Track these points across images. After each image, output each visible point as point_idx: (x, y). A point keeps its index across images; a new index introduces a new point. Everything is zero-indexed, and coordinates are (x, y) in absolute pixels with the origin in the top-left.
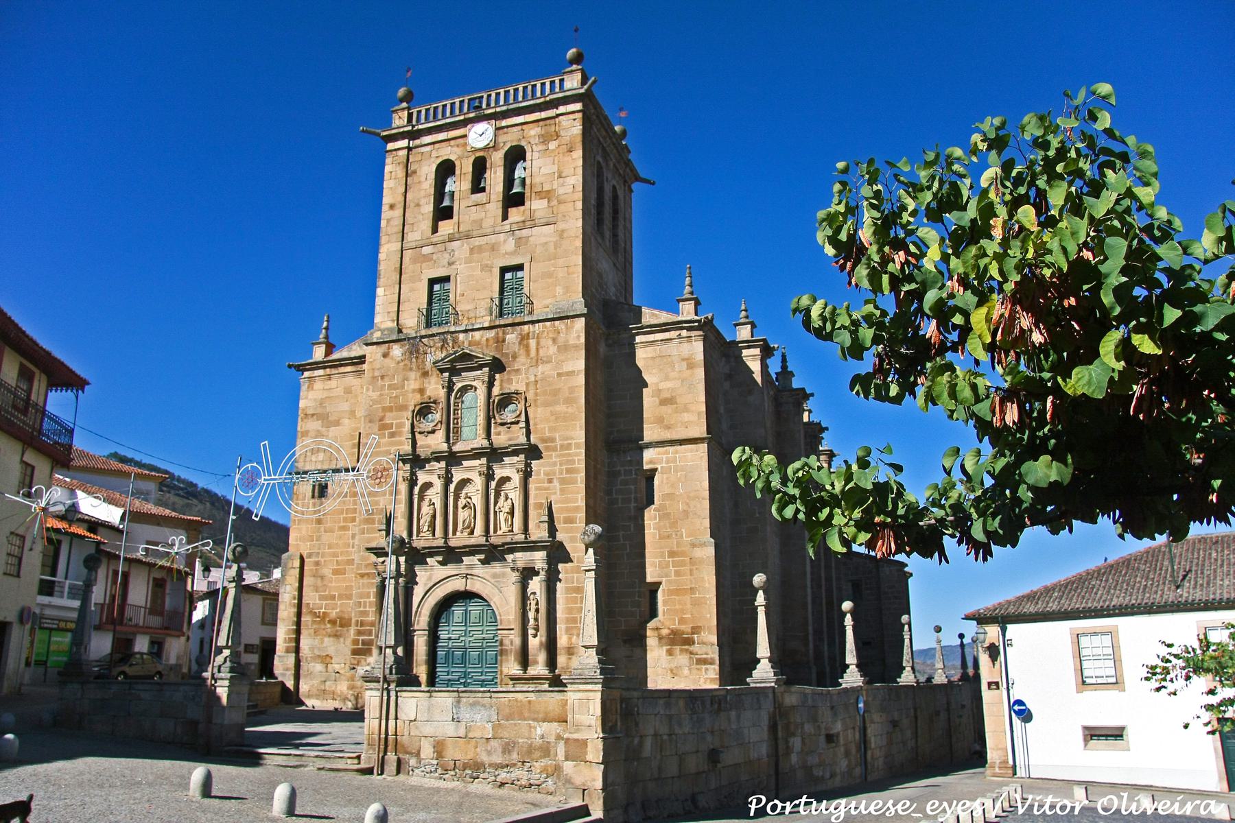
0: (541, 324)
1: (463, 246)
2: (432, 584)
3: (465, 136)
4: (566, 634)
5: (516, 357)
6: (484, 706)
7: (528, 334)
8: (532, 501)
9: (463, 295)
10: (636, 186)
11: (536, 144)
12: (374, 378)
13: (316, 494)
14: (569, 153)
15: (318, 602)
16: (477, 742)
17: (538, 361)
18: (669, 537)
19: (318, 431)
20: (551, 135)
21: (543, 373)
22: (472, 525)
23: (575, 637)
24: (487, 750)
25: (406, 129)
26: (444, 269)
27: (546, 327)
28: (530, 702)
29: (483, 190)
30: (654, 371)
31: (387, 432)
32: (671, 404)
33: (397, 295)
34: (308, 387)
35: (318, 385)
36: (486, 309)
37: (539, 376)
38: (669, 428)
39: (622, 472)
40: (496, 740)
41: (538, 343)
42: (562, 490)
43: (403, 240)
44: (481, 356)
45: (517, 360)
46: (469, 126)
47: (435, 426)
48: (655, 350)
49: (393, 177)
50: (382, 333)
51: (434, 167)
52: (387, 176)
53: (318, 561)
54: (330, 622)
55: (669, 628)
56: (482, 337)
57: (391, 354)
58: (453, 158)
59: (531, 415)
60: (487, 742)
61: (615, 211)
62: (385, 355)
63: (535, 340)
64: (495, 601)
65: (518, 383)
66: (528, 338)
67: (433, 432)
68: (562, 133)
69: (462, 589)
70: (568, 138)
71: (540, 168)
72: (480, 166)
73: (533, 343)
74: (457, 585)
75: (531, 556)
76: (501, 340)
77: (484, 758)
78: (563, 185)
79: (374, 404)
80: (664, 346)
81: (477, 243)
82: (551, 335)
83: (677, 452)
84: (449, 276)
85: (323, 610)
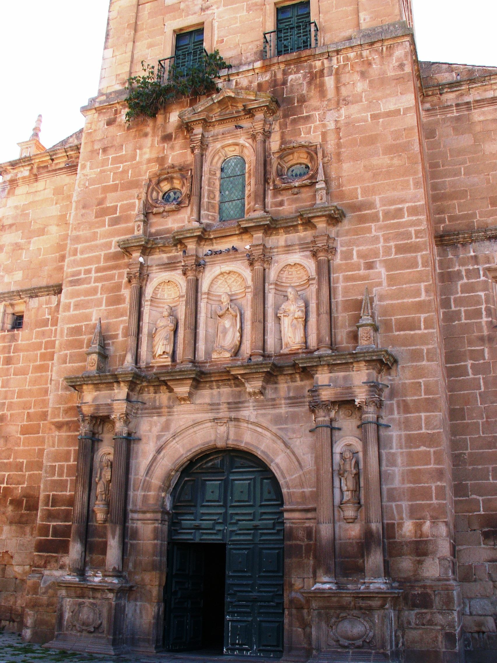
4: (411, 517)
5: (305, 101)
7: (322, 71)
9: (222, 41)
19: (16, 244)
21: (348, 117)
23: (428, 523)
26: (195, 16)
27: (347, 59)
31: (107, 218)
39: (464, 273)
41: (338, 81)
42: (391, 280)
44: (253, 98)
50: (107, 98)
54: (12, 502)
56: (251, 82)
59: (333, 175)
62: (110, 123)
63: (333, 77)
65: (309, 133)
73: (329, 82)
76: (279, 82)
79: (90, 184)
82: (358, 69)
84: (203, 23)
85: (5, 485)
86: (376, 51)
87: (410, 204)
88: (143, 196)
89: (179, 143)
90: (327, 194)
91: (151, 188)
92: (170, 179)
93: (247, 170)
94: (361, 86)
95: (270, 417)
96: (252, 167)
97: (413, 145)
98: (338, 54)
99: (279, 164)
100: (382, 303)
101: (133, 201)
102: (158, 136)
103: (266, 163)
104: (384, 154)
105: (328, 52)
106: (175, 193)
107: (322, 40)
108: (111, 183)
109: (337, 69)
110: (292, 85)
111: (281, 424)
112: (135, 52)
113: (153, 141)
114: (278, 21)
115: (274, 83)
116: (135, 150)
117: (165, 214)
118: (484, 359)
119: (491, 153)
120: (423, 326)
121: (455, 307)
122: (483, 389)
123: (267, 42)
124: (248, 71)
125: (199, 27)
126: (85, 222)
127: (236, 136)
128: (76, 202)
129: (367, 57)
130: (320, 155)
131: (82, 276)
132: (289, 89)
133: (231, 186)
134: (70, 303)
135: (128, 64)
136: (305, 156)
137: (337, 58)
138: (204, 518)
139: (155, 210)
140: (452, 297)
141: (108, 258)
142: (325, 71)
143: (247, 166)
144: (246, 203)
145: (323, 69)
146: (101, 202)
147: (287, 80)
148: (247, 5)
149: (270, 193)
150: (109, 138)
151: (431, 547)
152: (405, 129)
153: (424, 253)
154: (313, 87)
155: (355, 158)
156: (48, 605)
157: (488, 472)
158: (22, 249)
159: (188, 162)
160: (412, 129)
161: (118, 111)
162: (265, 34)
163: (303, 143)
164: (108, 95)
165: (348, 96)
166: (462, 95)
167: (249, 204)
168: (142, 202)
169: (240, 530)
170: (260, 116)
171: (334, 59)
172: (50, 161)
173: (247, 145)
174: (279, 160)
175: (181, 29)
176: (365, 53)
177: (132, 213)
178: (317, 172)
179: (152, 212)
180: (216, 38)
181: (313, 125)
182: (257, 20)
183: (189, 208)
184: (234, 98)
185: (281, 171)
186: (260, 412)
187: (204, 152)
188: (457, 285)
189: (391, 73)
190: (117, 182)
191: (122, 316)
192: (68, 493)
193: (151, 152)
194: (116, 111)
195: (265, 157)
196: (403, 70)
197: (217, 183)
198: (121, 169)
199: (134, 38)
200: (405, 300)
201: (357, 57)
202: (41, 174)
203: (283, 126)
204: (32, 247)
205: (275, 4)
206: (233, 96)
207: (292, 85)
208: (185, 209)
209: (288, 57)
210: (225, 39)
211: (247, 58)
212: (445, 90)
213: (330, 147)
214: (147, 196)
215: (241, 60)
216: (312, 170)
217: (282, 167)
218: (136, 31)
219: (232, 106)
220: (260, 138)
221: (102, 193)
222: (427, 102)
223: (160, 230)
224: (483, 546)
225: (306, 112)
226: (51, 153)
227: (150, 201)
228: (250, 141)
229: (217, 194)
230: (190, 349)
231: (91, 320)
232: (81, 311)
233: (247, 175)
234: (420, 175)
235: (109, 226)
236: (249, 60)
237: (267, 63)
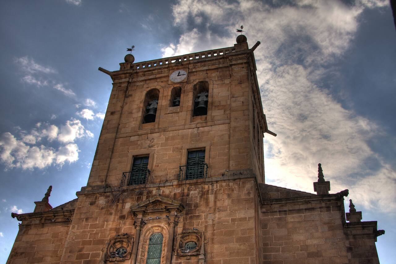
1: (161, 136)
3: (168, 76)
5: (198, 207)
11: (216, 81)
17: (216, 209)
21: (219, 218)
25: (128, 72)
27: (221, 186)
30: (301, 231)
32: (318, 257)
41: (216, 198)
44: (171, 203)
48: (301, 216)
50: (92, 189)
51: (144, 93)
57: (97, 203)
58: (158, 87)
59: (209, 250)
63: (213, 195)
65: (198, 225)
66: (208, 194)
72: (177, 93)
73: (211, 197)
76: (185, 194)
78: (235, 101)
79: (76, 239)
80: (308, 214)
81: (171, 135)
82: (226, 192)
84: (149, 154)
86: (237, 184)
88: (105, 250)
89: (129, 221)
90: (205, 261)
91: (110, 245)
92: (121, 242)
94: (227, 202)
96: (166, 241)
97: (252, 238)
98: (217, 183)
99: (181, 241)
101: (99, 252)
102: (118, 215)
103: (174, 240)
104: (237, 242)
105: (212, 181)
106: (123, 250)
107: (210, 174)
108: (88, 239)
109: (216, 191)
110: (192, 197)
112: (111, 164)
113: (115, 218)
114: (188, 159)
115: (183, 194)
116: (104, 222)
117: (116, 262)
119: (296, 240)
123: (181, 170)
124: (170, 186)
125: (147, 156)
126: (70, 261)
127: (160, 222)
128: (66, 248)
129: (232, 186)
130: (203, 239)
132: (190, 199)
133: (154, 249)
135: (106, 171)
136: (195, 238)
137: (217, 185)
139: (110, 259)
142: (210, 191)
143: (164, 239)
144: (161, 261)
145: (209, 190)
146: (81, 250)
147: (189, 194)
148: (173, 147)
149: (174, 257)
150: (91, 212)
152: (248, 229)
154: (202, 199)
155: (221, 242)
159: (133, 233)
160: (252, 229)
161: (97, 198)
162: (180, 167)
164: (93, 187)
165: (220, 207)
166: (282, 206)
167: (163, 262)
168: (104, 253)
170: (174, 213)
171: (215, 185)
172: (53, 217)
173: (165, 228)
174: (181, 239)
175: (137, 156)
176: (231, 184)
177: (98, 259)
178: (200, 248)
179: (109, 260)
180: (155, 164)
181: (201, 221)
182: (177, 157)
183: (130, 261)
184: (161, 201)
185: (182, 244)
187: (142, 229)
189: (243, 197)
190: (92, 239)
193: (113, 224)
194: (96, 197)
195: (174, 235)
196: (250, 196)
197: (147, 247)
198: (94, 232)
199: (111, 157)
201: (226, 185)
202: (46, 223)
203: (185, 219)
205: (188, 149)
206: (160, 200)
207: (192, 197)
208: (127, 261)
209: (191, 181)
210: (160, 165)
211: (170, 177)
212: (274, 203)
213: (209, 234)
214: (107, 250)
215: (167, 178)
216: (198, 246)
217: (183, 243)
218: (112, 152)
219: (159, 204)
220: (172, 225)
221: (82, 245)
222: (264, 208)
225: (198, 213)
226: (55, 212)
227: (109, 254)
228: (167, 225)
229: (146, 253)
233: (163, 245)
234: (255, 256)
236: (171, 179)
237: (180, 183)
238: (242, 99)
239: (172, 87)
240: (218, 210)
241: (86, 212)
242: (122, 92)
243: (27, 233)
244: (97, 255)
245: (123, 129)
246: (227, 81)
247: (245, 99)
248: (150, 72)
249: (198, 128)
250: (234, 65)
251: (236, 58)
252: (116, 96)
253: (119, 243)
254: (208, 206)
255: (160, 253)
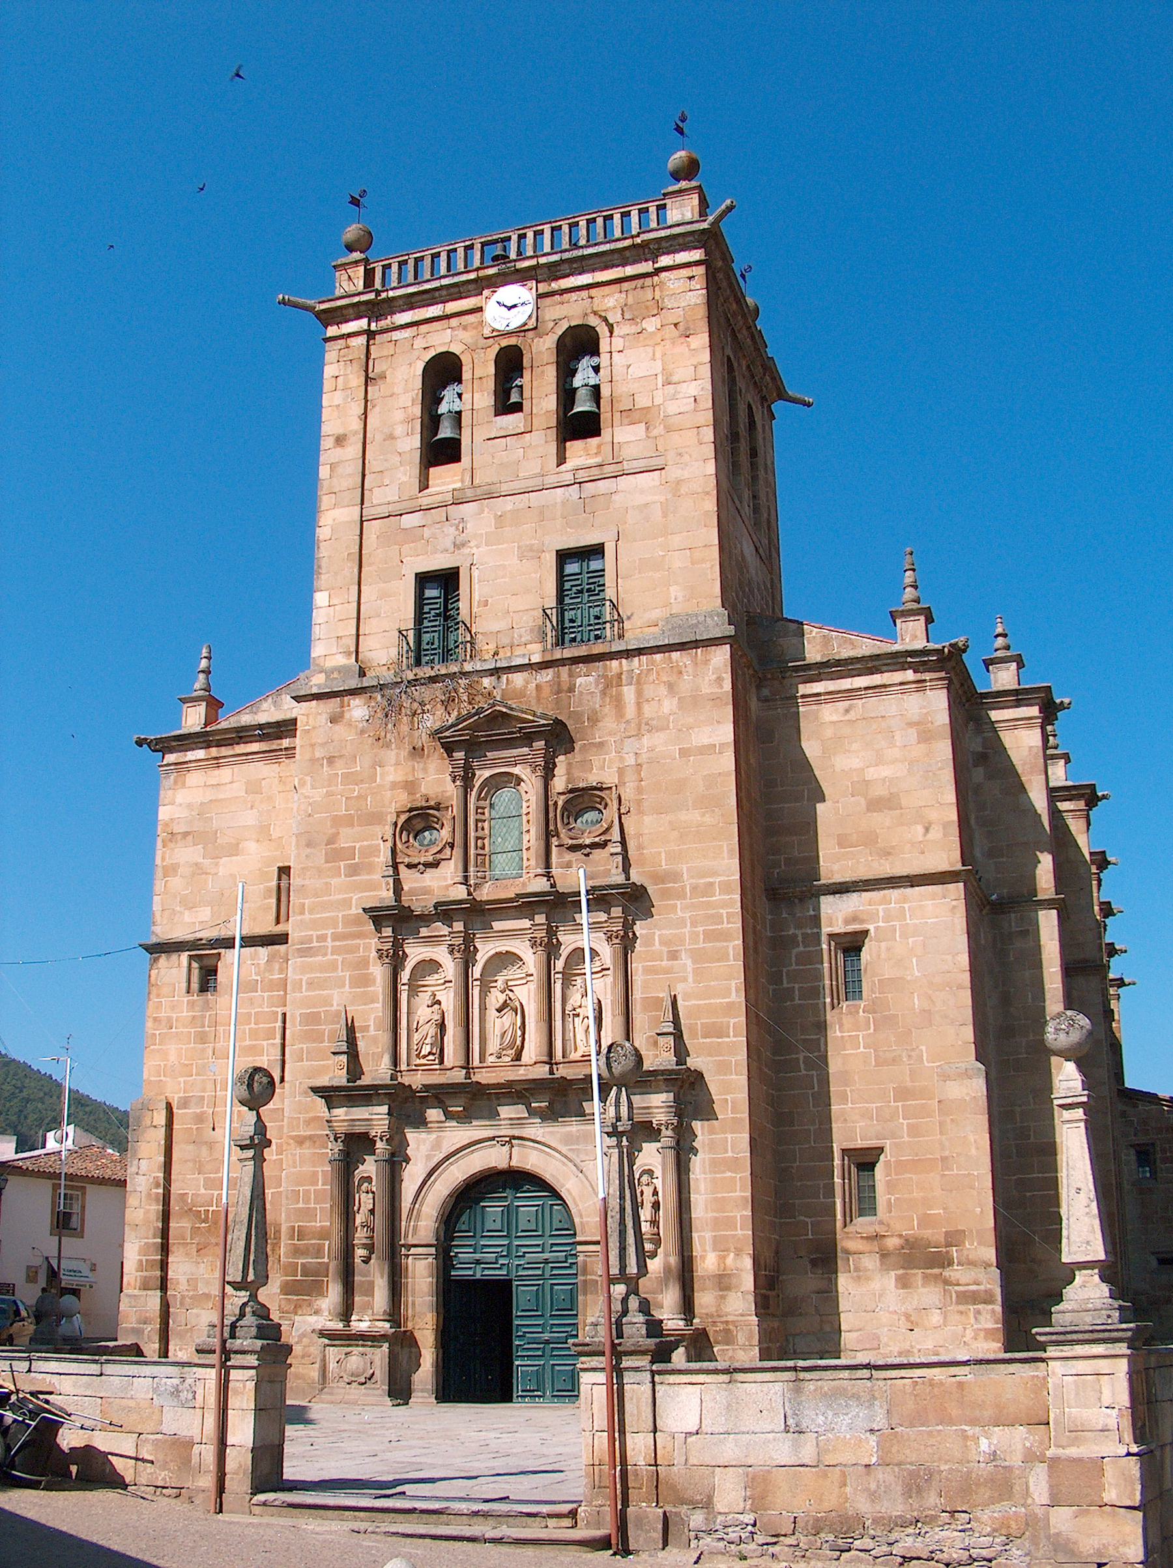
0: (644, 658)
2: (442, 1156)
3: (480, 309)
6: (856, 1397)
7: (620, 675)
8: (637, 994)
9: (486, 604)
10: (778, 407)
12: (313, 760)
13: (195, 986)
14: (683, 340)
15: (203, 1191)
16: (843, 1474)
17: (643, 726)
18: (894, 1061)
19: (196, 864)
20: (647, 307)
22: (519, 1042)
24: (867, 1489)
28: (960, 1385)
29: (517, 408)
30: (855, 746)
31: (342, 864)
32: (890, 809)
33: (355, 604)
34: (176, 782)
35: (195, 778)
36: (532, 631)
37: (644, 758)
38: (889, 854)
39: (800, 938)
40: (888, 1469)
41: (639, 693)
43: (362, 503)
44: (531, 718)
45: (600, 724)
46: (486, 292)
47: (440, 852)
49: (340, 386)
50: (327, 677)
51: (420, 367)
52: (327, 385)
53: (203, 1113)
55: (900, 1236)
57: (347, 715)
58: (456, 349)
59: (630, 830)
60: (868, 1474)
61: (754, 453)
62: (334, 720)
63: (633, 688)
64: (568, 1186)
65: (603, 768)
67: (435, 865)
68: (668, 303)
69: (502, 1164)
70: (680, 312)
71: (629, 367)
74: (494, 1158)
75: (643, 1100)
77: (863, 1506)
78: (674, 398)
81: (509, 507)
83: (905, 900)
85: (214, 1208)
87: (722, 878)
93: (524, 811)
94: (669, 705)
95: (558, 1136)
97: (728, 798)
100: (687, 1003)
101: (377, 842)
105: (627, 650)
110: (581, 693)
111: (572, 1144)
113: (398, 755)
118: (819, 1051)
120: (732, 1034)
121: (788, 983)
122: (816, 1089)
131: (315, 944)
133: (505, 830)
134: (301, 979)
138: (484, 1250)
140: (785, 970)
141: (348, 921)
143: (525, 805)
144: (525, 859)
151: (734, 1281)
153: (736, 942)
155: (659, 811)
156: (303, 1357)
157: (819, 1188)
158: (207, 874)
159: (448, 794)
163: (594, 784)
165: (652, 719)
169: (528, 1263)
177: (377, 860)
182: (533, 575)
183: (452, 861)
186: (547, 1129)
188: (790, 953)
189: (706, 689)
191: (372, 1002)
192: (318, 1225)
196: (722, 687)
198: (356, 794)
200: (712, 1001)
204: (222, 871)
215: (513, 637)
221: (332, 827)
223: (415, 888)
224: (810, 1275)
230: (462, 1053)
231: (332, 1005)
232: (317, 992)
235: (346, 876)
236: (523, 639)
238: (692, 389)
239: (496, 348)
240: (647, 727)
241: (326, 743)
242: (355, 363)
243: (184, 785)
244: (375, 851)
245: (376, 490)
246: (651, 325)
247: (702, 389)
248: (425, 296)
249: (580, 483)
250: (665, 271)
251: (671, 246)
252: (340, 379)
253: (419, 820)
254: (622, 716)
255: (521, 841)
